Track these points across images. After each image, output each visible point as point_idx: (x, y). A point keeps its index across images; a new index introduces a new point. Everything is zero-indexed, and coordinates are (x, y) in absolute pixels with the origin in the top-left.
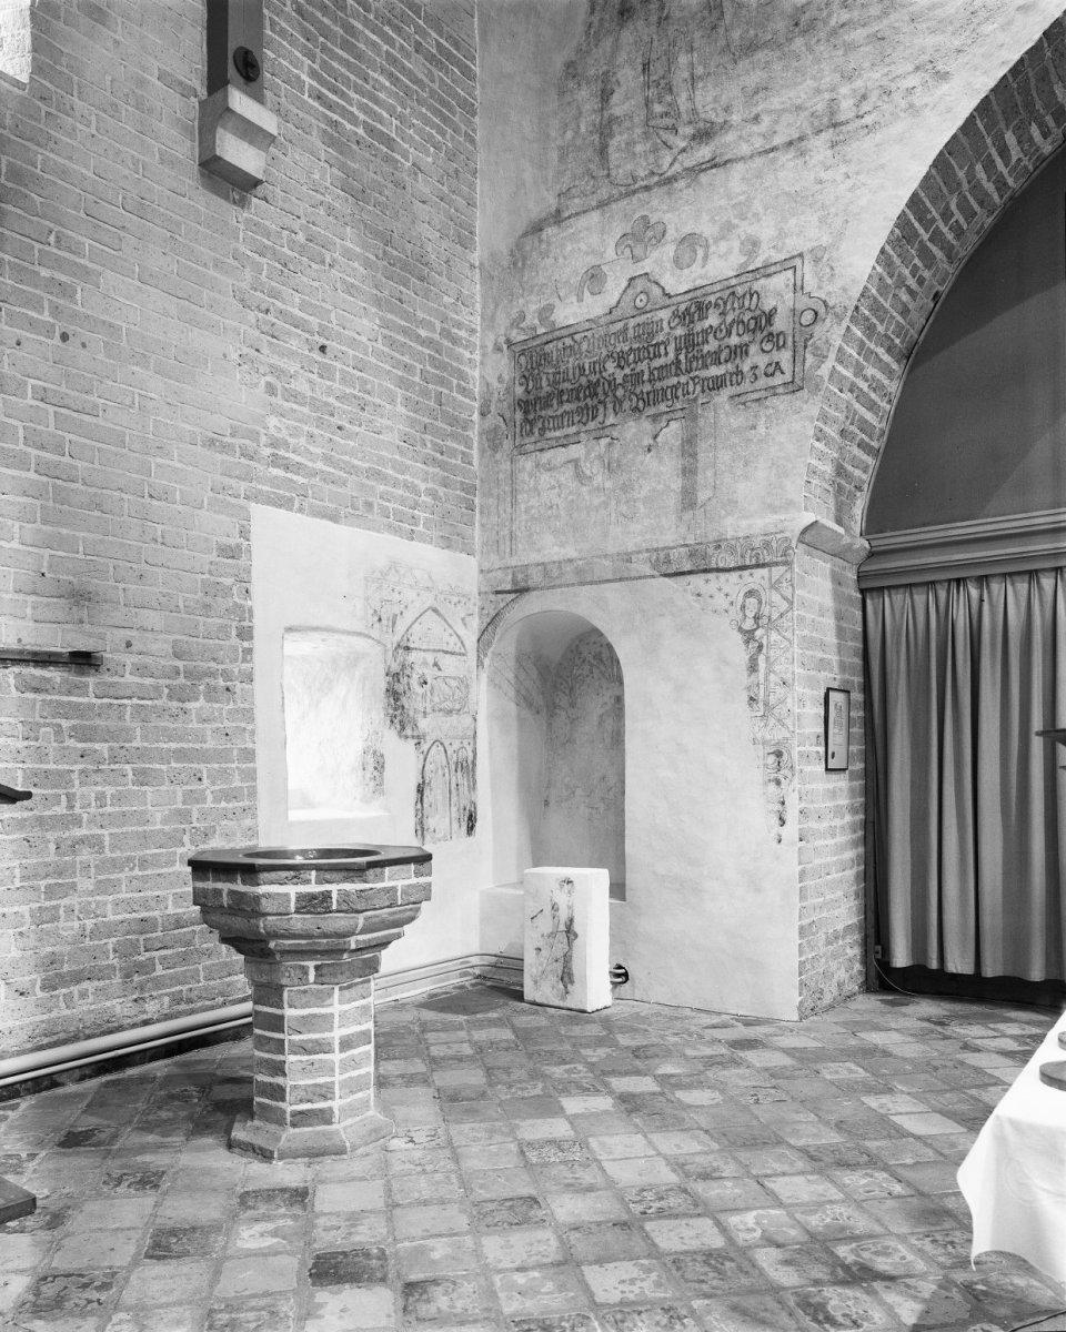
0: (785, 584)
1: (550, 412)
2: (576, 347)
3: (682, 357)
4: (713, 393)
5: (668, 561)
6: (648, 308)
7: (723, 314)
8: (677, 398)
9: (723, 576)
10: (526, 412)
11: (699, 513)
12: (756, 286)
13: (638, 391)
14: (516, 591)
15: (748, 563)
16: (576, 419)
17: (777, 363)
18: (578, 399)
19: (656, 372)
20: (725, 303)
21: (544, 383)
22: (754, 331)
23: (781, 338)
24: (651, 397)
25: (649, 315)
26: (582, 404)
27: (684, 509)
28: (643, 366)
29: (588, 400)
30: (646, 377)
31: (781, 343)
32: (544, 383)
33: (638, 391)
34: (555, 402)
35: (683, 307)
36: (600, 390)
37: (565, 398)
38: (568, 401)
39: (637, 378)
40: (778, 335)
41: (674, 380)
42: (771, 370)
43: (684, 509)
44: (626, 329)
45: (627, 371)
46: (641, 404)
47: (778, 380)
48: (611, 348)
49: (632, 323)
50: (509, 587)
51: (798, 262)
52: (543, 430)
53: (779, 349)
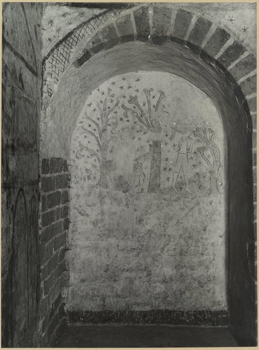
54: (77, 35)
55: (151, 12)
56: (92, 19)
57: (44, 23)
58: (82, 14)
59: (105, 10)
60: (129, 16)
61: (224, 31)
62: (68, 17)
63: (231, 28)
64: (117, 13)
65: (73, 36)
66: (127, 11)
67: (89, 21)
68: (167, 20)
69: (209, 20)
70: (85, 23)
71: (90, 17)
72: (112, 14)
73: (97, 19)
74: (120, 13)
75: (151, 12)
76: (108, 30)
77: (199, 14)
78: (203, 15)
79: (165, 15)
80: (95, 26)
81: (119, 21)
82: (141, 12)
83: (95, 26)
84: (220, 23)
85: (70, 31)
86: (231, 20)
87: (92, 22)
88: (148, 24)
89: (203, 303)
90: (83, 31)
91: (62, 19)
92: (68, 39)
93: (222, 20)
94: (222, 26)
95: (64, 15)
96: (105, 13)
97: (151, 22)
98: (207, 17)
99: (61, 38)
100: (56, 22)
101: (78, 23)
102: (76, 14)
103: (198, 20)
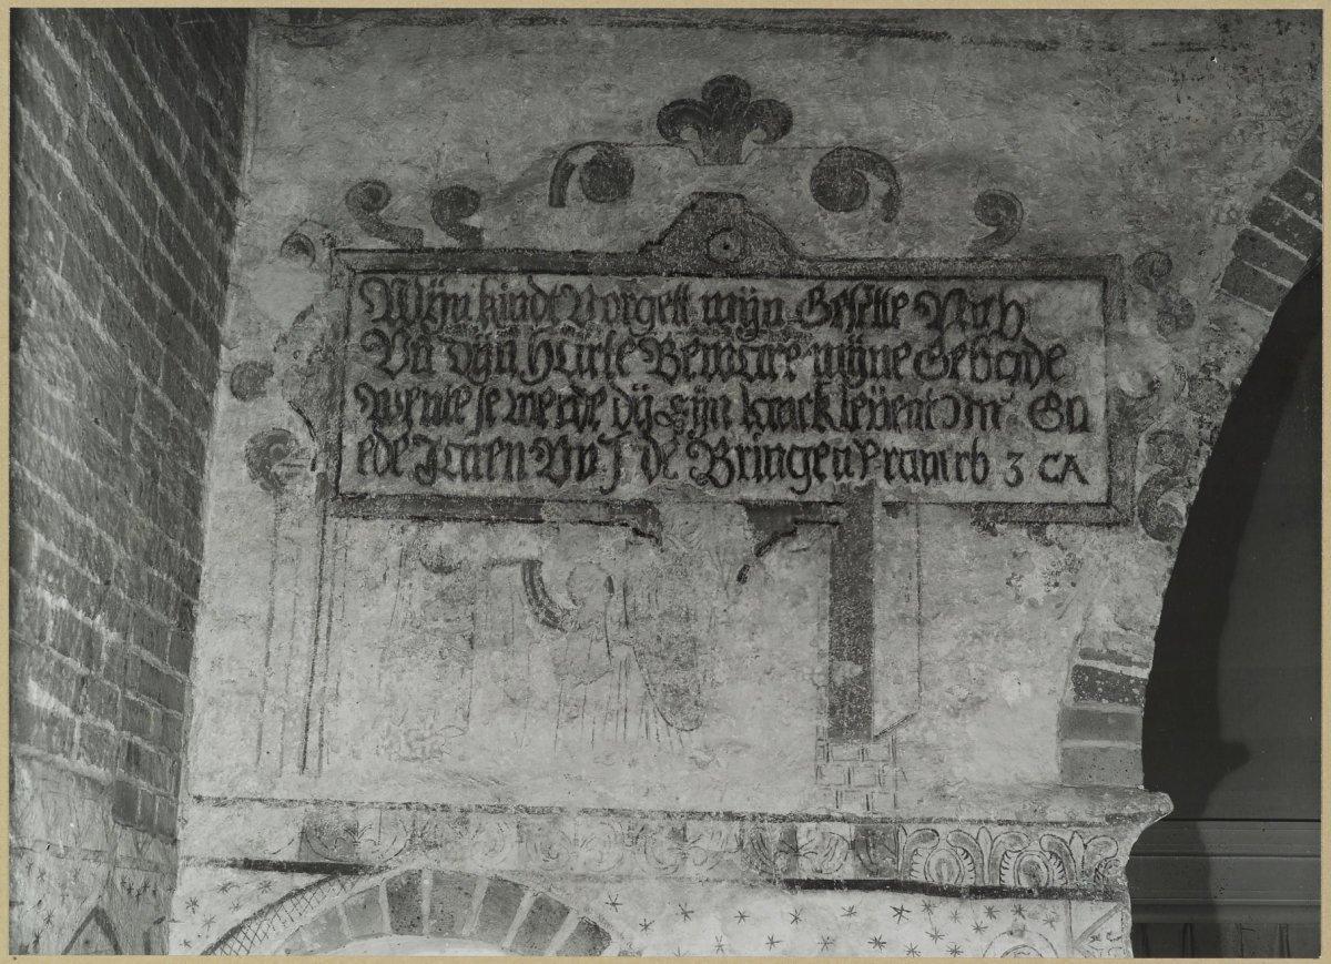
0: (1105, 943)
1: (450, 433)
2: (541, 304)
3: (833, 389)
4: (914, 487)
5: (792, 848)
6: (743, 267)
7: (936, 325)
8: (821, 477)
9: (944, 908)
10: (379, 418)
11: (878, 751)
12: (1013, 294)
13: (713, 439)
14: (308, 868)
15: (1010, 882)
16: (532, 466)
17: (1070, 459)
18: (543, 424)
19: (762, 409)
20: (941, 309)
21: (441, 360)
22: (1012, 379)
23: (1078, 408)
24: (750, 459)
25: (748, 284)
26: (552, 434)
27: (836, 732)
28: (732, 388)
29: (570, 429)
30: (736, 412)
31: (1078, 420)
32: (441, 360)
33: (713, 439)
34: (470, 414)
35: (834, 289)
36: (604, 414)
37: (502, 408)
38: (509, 418)
39: (712, 412)
40: (1071, 402)
41: (811, 439)
42: (1053, 469)
43: (836, 732)
44: (680, 299)
45: (684, 389)
46: (721, 471)
47: (1071, 490)
48: (638, 328)
49: (699, 287)
50: (288, 854)
52: (429, 469)
53: (1072, 430)
54: (250, 934)
55: (427, 882)
56: (289, 896)
57: (177, 906)
58: (267, 885)
59: (320, 877)
60: (374, 890)
61: (596, 927)
62: (233, 891)
63: (613, 922)
64: (348, 885)
65: (241, 935)
66: (372, 879)
67: (281, 902)
68: (465, 900)
69: (562, 901)
70: (271, 907)
71: (286, 892)
72: (337, 887)
73: (299, 897)
74: (353, 885)
75: (427, 882)
76: (323, 921)
77: (539, 889)
78: (550, 890)
79: (460, 889)
80: (295, 915)
81: (352, 902)
82: (404, 882)
83: (295, 915)
84: (587, 909)
85: (235, 924)
86: (614, 904)
87: (288, 905)
88: (418, 909)
89: (492, 533)
90: (265, 926)
91: (220, 896)
92: (230, 942)
93: (592, 904)
94: (593, 917)
95: (224, 889)
96: (319, 883)
97: (425, 907)
98: (556, 896)
99: (213, 940)
100: (203, 903)
101: (257, 908)
102: (253, 887)
103: (536, 902)
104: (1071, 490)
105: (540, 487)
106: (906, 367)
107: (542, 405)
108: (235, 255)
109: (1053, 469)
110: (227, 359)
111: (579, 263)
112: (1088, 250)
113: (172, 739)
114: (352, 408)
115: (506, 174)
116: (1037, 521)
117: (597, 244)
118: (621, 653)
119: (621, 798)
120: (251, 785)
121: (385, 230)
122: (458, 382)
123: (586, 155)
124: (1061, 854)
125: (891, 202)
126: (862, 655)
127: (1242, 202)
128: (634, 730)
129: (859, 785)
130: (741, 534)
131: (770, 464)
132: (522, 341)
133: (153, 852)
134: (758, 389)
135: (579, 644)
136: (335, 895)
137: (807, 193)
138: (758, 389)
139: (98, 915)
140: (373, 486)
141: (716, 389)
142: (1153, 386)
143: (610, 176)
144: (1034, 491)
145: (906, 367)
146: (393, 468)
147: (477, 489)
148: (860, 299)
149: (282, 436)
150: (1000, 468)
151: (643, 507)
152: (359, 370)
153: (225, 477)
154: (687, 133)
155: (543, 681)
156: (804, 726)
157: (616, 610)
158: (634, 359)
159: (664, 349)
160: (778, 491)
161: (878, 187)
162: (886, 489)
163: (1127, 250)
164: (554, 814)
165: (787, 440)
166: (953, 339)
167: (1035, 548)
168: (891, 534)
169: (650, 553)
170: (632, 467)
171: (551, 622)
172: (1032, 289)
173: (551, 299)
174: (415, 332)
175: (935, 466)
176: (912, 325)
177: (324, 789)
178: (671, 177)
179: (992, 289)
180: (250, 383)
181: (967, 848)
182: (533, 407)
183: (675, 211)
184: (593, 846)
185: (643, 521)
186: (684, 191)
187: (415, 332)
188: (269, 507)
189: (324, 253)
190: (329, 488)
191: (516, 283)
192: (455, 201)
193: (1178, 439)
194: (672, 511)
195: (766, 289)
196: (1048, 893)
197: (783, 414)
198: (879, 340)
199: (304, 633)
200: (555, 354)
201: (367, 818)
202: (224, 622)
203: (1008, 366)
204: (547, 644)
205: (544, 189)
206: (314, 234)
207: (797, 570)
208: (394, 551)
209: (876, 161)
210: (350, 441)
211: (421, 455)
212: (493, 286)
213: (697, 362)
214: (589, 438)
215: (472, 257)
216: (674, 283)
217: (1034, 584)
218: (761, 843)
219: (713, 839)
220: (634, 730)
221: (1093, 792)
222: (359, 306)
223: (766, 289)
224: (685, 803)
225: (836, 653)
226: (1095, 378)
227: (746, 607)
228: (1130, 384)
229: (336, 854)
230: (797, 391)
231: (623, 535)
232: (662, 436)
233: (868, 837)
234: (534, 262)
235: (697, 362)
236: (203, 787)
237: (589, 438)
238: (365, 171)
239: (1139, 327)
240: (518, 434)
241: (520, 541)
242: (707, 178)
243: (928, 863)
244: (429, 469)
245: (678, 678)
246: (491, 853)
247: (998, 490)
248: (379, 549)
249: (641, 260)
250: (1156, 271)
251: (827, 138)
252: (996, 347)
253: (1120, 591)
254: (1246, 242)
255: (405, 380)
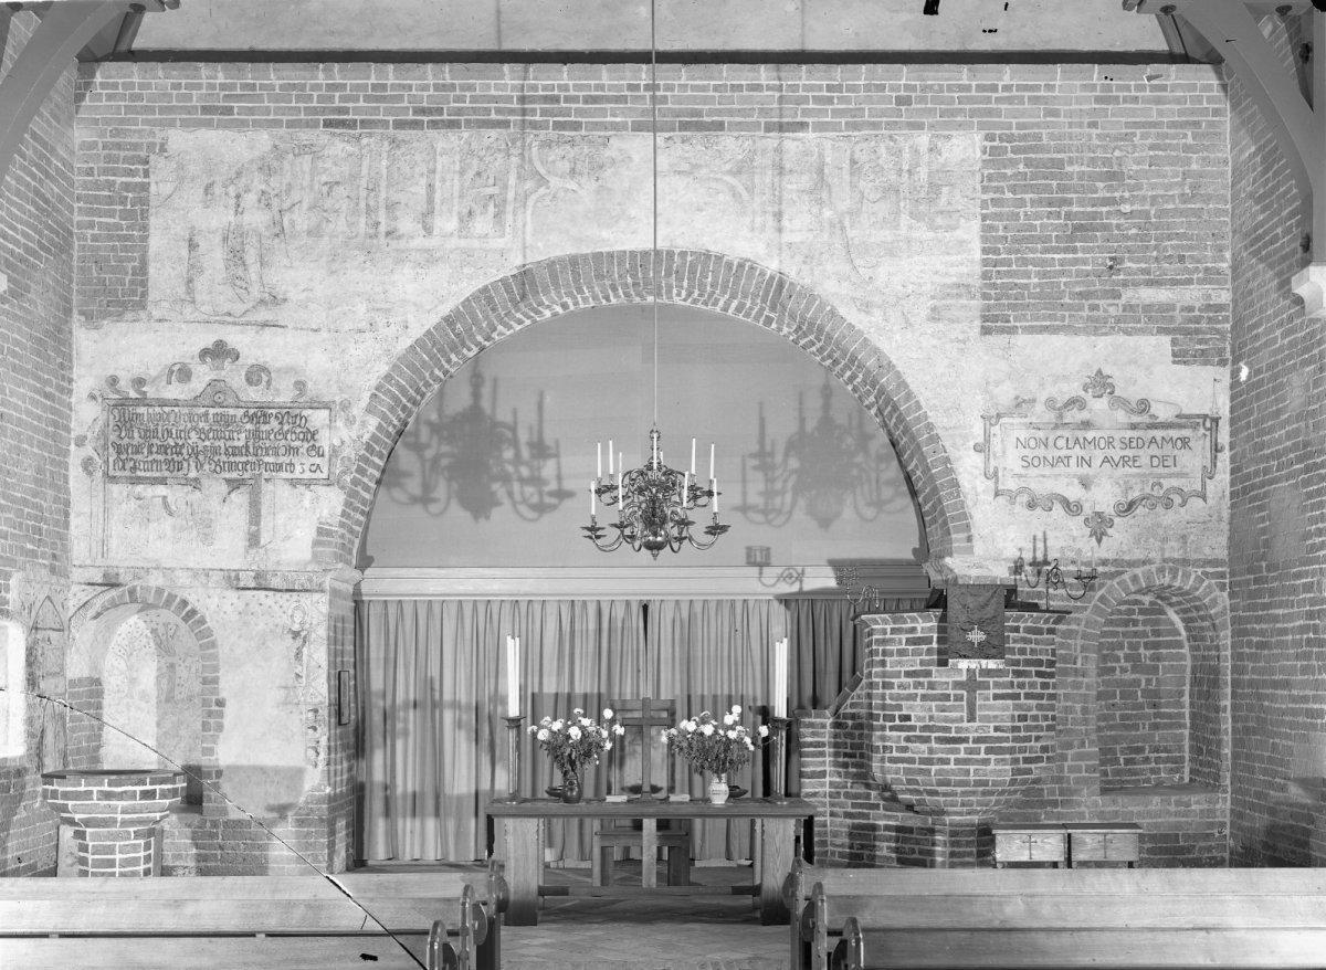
1: (139, 457)
3: (250, 444)
5: (238, 579)
7: (281, 423)
10: (119, 453)
11: (262, 551)
12: (305, 413)
16: (164, 467)
21: (136, 435)
26: (169, 458)
27: (250, 546)
28: (221, 443)
32: (136, 435)
34: (145, 451)
35: (251, 411)
36: (184, 451)
37: (154, 449)
39: (216, 451)
41: (244, 459)
42: (314, 468)
43: (250, 546)
44: (206, 414)
45: (207, 443)
46: (218, 469)
47: (318, 475)
49: (212, 411)
50: (100, 581)
51: (333, 406)
52: (134, 468)
104: (318, 475)
105: (167, 474)
106: (272, 437)
107: (166, 449)
108: (73, 400)
109: (314, 468)
110: (73, 435)
111: (176, 403)
112: (326, 399)
113: (65, 549)
114: (111, 449)
115: (153, 373)
116: (308, 484)
117: (182, 397)
118: (191, 523)
119: (191, 565)
120: (88, 562)
121: (118, 392)
122: (142, 441)
123: (176, 368)
124: (310, 580)
125: (269, 383)
126: (258, 524)
127: (374, 382)
128: (194, 545)
129: (257, 561)
130: (224, 488)
131: (232, 466)
132: (160, 428)
133: (62, 581)
134: (229, 443)
135: (179, 521)
136: (114, 593)
137: (243, 377)
138: (229, 443)
139: (48, 597)
140: (118, 474)
141: (217, 443)
142: (343, 442)
143: (184, 374)
144: (308, 475)
145: (272, 437)
146: (124, 468)
147: (148, 474)
148: (260, 414)
149: (90, 459)
150: (298, 468)
151: (196, 479)
152: (113, 437)
153: (75, 472)
154: (208, 360)
155: (169, 533)
156: (242, 543)
157: (189, 511)
158: (193, 434)
159: (202, 431)
160: (234, 475)
161: (265, 378)
162: (266, 475)
163: (338, 399)
164: (172, 570)
165: (237, 459)
166: (286, 428)
167: (307, 492)
168: (267, 488)
169: (197, 492)
170: (193, 465)
171: (171, 514)
172: (310, 412)
173: (168, 415)
174: (128, 425)
175: (279, 467)
176: (274, 424)
177: (109, 563)
178: (203, 374)
179: (298, 411)
180: (81, 441)
181: (285, 579)
182: (164, 449)
183: (204, 386)
184: (183, 578)
185: (196, 484)
186: (207, 379)
187: (128, 425)
188: (89, 480)
189: (100, 400)
190: (106, 474)
191: (158, 409)
192: (139, 382)
193: (349, 459)
194: (205, 482)
195: (231, 411)
196: (307, 591)
197: (236, 451)
198: (264, 428)
199: (101, 515)
200: (169, 432)
201: (121, 571)
202: (78, 515)
203: (301, 436)
204: (170, 520)
205: (165, 378)
206: (97, 393)
207: (240, 498)
208: (125, 494)
209: (263, 369)
210: (111, 460)
211: (132, 464)
212: (151, 410)
213: (211, 435)
214: (180, 458)
215: (143, 400)
216: (203, 410)
217: (307, 503)
218: (230, 577)
219: (216, 577)
220: (194, 545)
221: (319, 563)
222: (111, 417)
223: (231, 411)
224: (209, 566)
225: (251, 523)
226: (325, 440)
227: (226, 509)
228: (336, 442)
229: (113, 581)
230: (241, 443)
231: (190, 488)
232: (201, 458)
233: (258, 576)
234: (163, 403)
235: (211, 435)
236: (75, 563)
237: (180, 458)
238: (111, 372)
239: (340, 424)
240: (160, 457)
241: (161, 490)
242: (213, 376)
243: (275, 582)
244: (134, 468)
245: (206, 531)
246: (156, 580)
247: (297, 475)
248: (121, 493)
249: (194, 402)
250: (345, 406)
251: (251, 361)
252: (298, 430)
253: (331, 503)
254: (374, 396)
255: (126, 440)
